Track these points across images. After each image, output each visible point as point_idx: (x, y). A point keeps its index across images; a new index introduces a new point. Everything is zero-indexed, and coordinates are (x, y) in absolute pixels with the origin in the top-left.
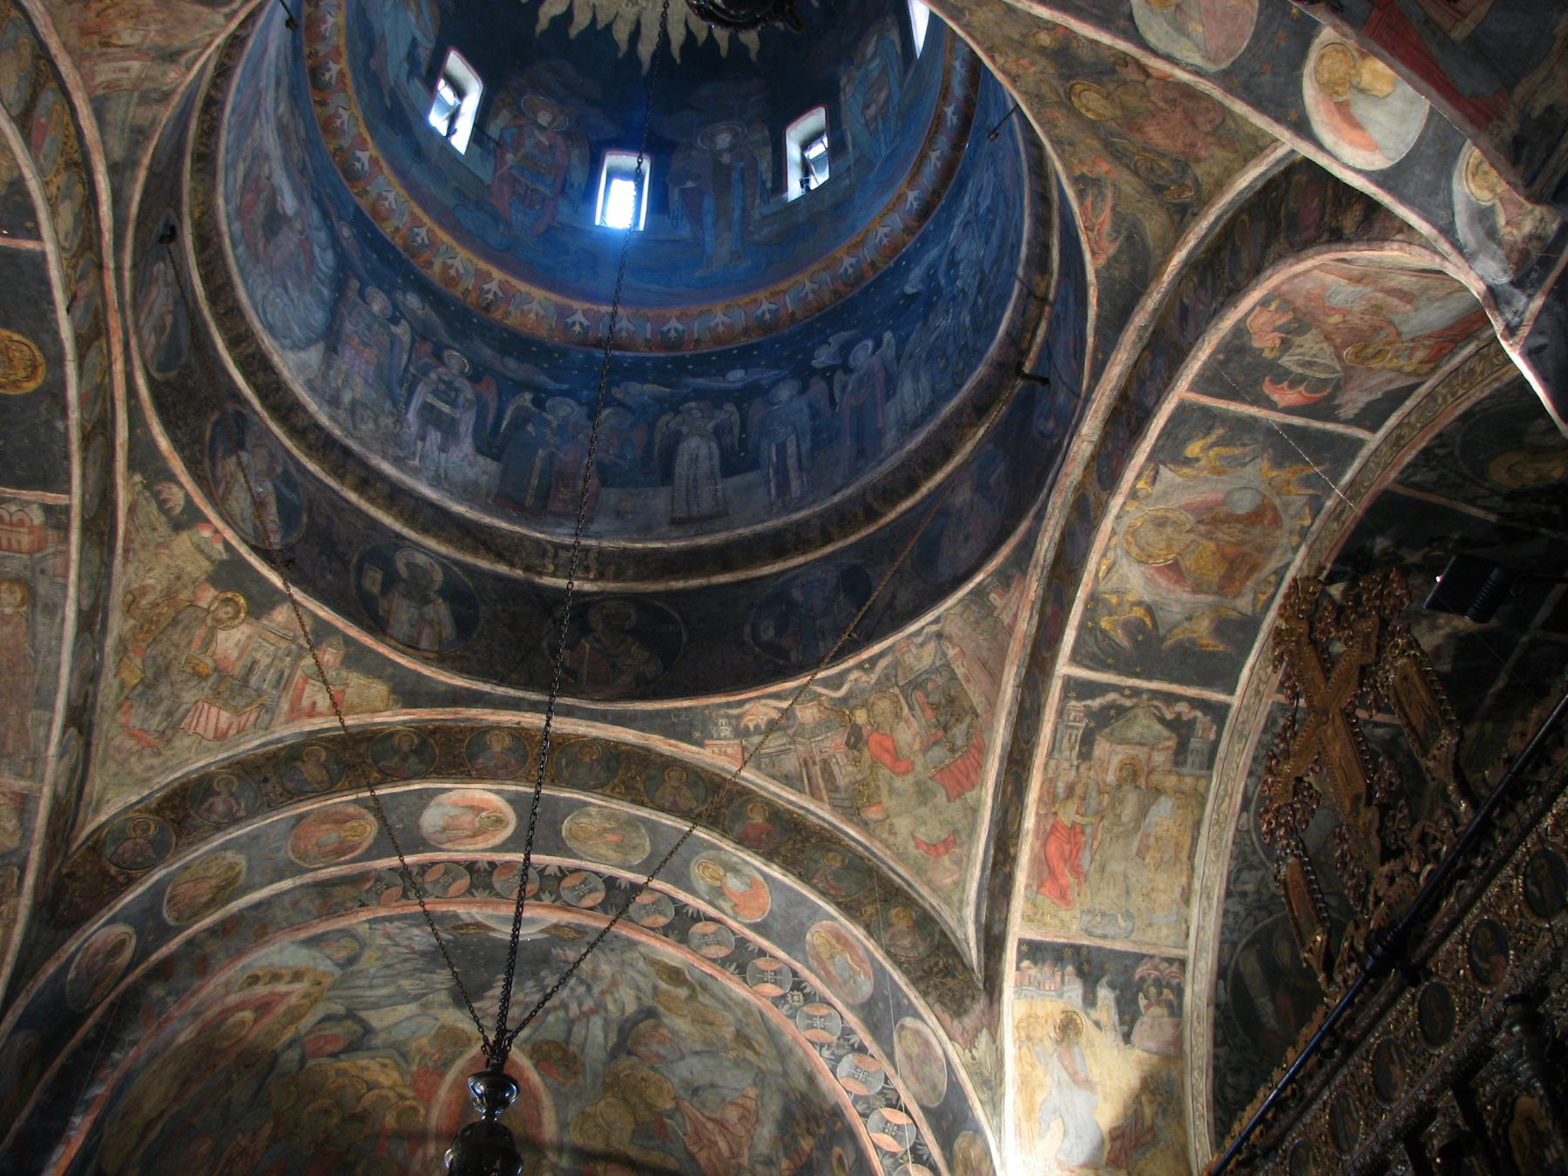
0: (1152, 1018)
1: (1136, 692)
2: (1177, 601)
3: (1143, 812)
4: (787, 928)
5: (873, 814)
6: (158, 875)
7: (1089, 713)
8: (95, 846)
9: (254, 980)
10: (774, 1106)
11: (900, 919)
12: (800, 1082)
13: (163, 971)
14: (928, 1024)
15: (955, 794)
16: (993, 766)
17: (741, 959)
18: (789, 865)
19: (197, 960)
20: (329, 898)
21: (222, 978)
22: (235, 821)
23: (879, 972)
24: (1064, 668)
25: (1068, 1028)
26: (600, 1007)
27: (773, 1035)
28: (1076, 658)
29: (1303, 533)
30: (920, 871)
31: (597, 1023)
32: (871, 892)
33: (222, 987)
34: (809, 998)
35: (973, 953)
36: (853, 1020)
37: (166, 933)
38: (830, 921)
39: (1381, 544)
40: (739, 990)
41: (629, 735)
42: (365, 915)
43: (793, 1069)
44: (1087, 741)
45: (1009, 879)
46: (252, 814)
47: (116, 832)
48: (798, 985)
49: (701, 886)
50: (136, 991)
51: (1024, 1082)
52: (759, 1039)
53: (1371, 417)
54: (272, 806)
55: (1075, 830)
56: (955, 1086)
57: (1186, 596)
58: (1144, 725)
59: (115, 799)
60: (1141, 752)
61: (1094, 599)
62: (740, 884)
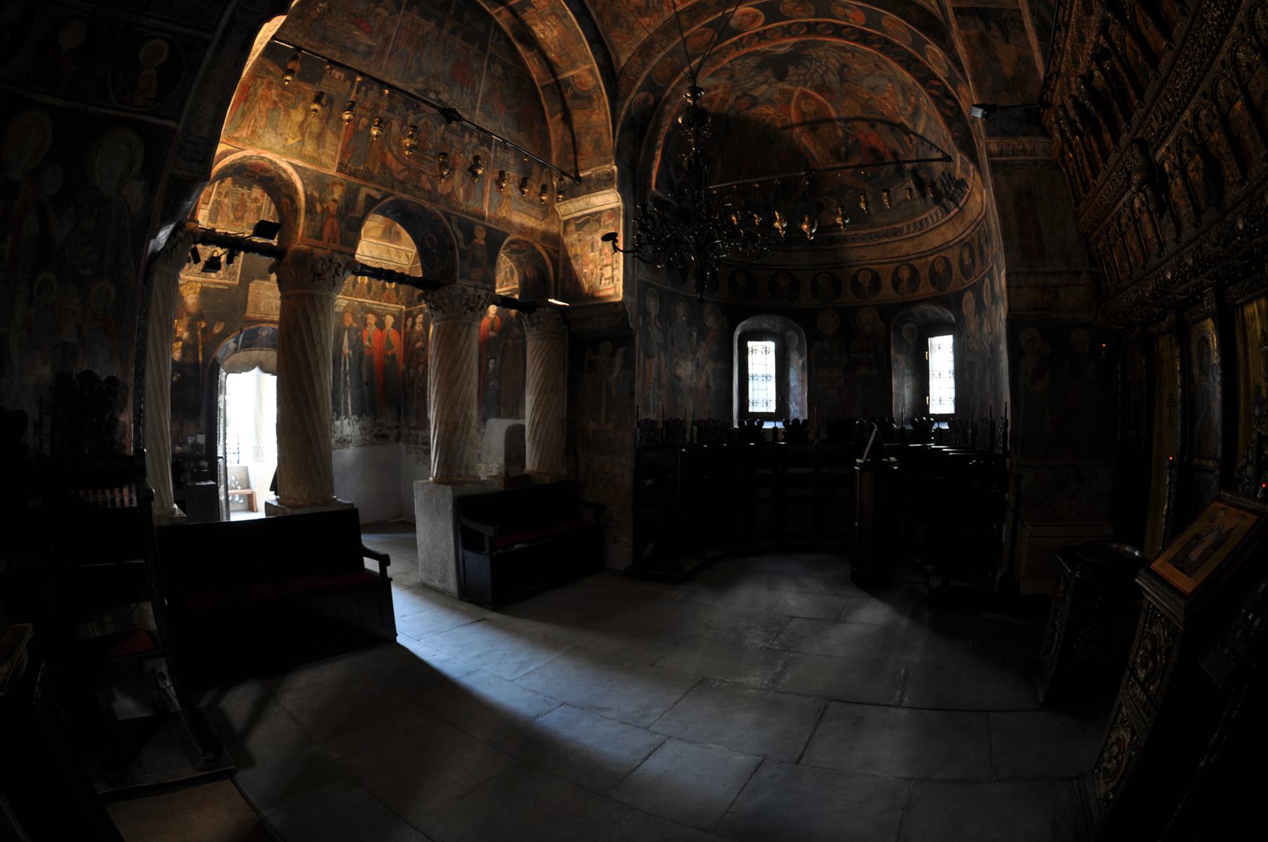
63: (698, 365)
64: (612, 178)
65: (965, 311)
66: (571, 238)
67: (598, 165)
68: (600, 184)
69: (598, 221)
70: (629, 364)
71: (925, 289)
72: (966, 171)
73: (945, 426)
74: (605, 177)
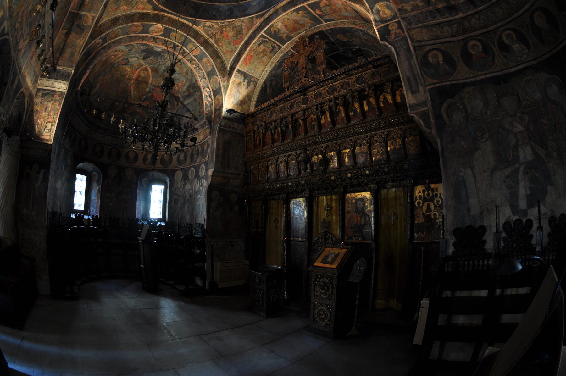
0: (251, 86)
1: (270, 40)
2: (284, 30)
3: (263, 57)
4: (200, 58)
5: (220, 44)
6: (108, 31)
7: (262, 40)
8: (100, 26)
9: (116, 51)
10: (188, 84)
11: (218, 60)
12: (194, 81)
13: (104, 48)
14: (219, 78)
15: (235, 45)
16: (243, 43)
17: (191, 61)
18: (204, 48)
19: (109, 47)
20: (131, 39)
21: (112, 50)
22: (122, 24)
23: (213, 68)
24: (262, 33)
25: (239, 84)
26: (165, 63)
27: (192, 73)
28: (265, 32)
29: (306, 30)
30: (224, 54)
31: (164, 66)
32: (216, 55)
33: (111, 52)
34: (200, 69)
35: (228, 69)
36: (205, 74)
37: (106, 42)
38: (208, 58)
39: (317, 36)
40: (189, 65)
41: (186, 22)
42: (136, 43)
43: (194, 79)
44: (260, 44)
45: (239, 60)
46: (125, 23)
47: (104, 24)
48: (198, 66)
49: (188, 48)
50: (99, 51)
51: (231, 90)
52: (190, 73)
53: (326, 21)
54: (128, 23)
55: (252, 56)
56: (220, 88)
57: (285, 30)
58: (269, 45)
59: (106, 19)
60: (267, 49)
61: (272, 25)
62: (195, 48)
63: (62, 184)
64: (69, 77)
65: (175, 178)
66: (38, 100)
67: (67, 66)
68: (61, 77)
69: (53, 96)
70: (46, 179)
71: (158, 165)
72: (202, 126)
73: (163, 224)
74: (66, 74)
